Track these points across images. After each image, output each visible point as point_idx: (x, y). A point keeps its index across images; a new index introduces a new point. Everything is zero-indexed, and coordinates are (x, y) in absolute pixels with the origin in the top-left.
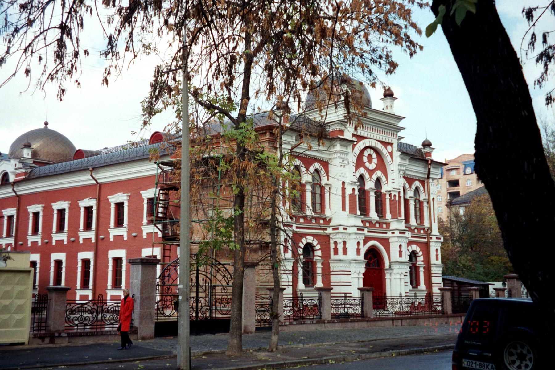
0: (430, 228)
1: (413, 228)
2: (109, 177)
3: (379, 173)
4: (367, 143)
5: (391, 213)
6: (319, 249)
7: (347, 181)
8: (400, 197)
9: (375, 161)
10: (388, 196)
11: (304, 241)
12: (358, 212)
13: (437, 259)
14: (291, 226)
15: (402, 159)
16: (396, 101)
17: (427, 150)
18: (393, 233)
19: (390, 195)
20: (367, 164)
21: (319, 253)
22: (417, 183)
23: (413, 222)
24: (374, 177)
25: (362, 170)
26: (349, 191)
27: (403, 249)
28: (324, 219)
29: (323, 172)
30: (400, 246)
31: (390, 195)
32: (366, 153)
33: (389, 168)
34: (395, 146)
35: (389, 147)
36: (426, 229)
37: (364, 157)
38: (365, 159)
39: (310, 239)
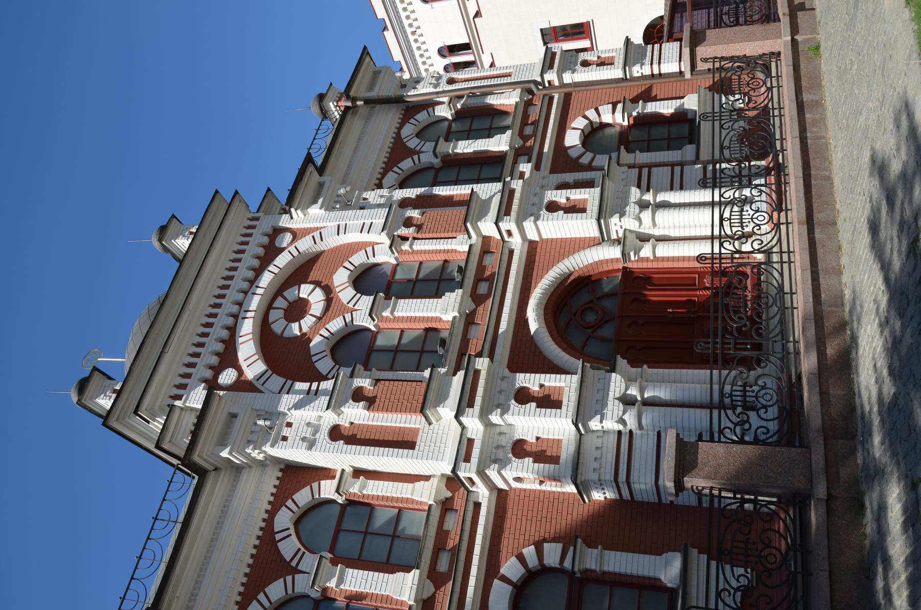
1: (518, 143)
4: (247, 327)
7: (330, 418)
15: (314, 202)
18: (509, 233)
22: (408, 130)
24: (346, 294)
28: (446, 506)
29: (303, 497)
33: (332, 241)
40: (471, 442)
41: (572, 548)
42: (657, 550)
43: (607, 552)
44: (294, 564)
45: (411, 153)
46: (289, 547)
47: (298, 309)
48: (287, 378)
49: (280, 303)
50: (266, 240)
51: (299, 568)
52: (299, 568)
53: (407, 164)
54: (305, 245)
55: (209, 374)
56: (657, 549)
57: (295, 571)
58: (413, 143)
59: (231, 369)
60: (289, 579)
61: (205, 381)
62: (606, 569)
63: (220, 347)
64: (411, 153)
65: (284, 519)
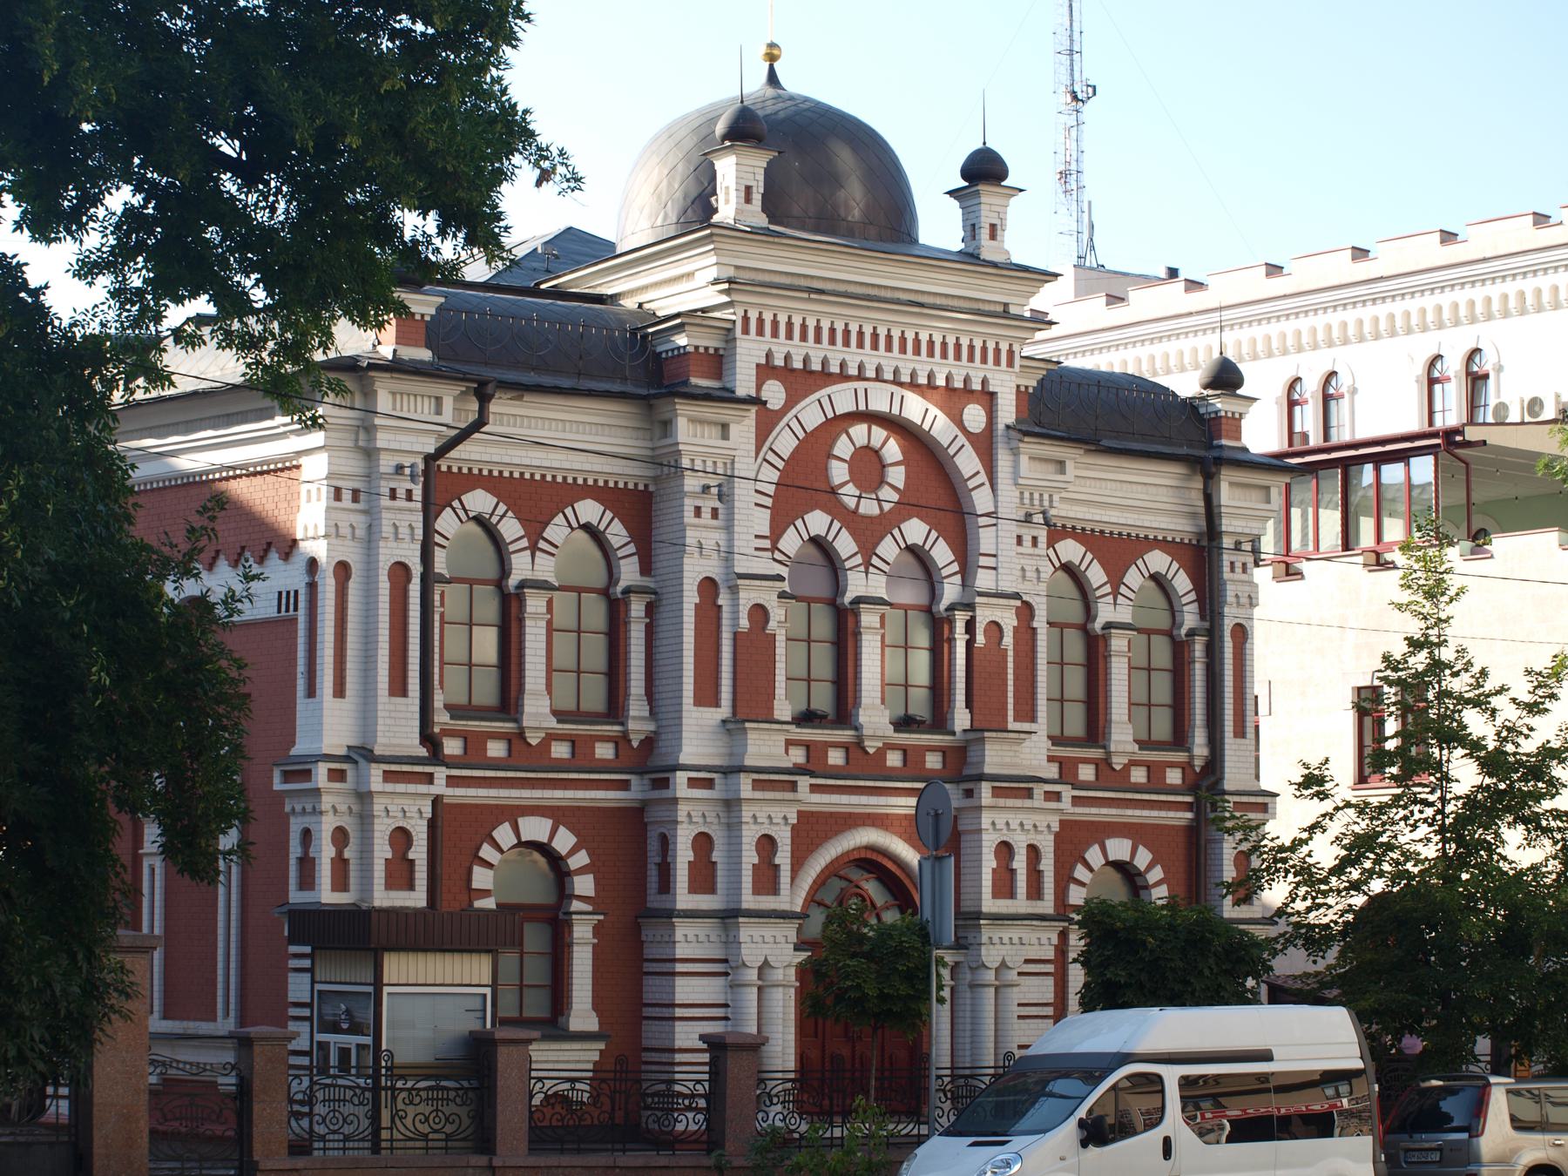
0: (1215, 763)
1: (1118, 762)
3: (915, 530)
4: (843, 398)
5: (969, 704)
6: (582, 871)
8: (1026, 632)
9: (897, 476)
10: (960, 627)
14: (429, 779)
16: (1015, 202)
17: (1221, 404)
19: (970, 626)
21: (584, 885)
22: (1158, 561)
23: (1122, 737)
25: (817, 521)
27: (1020, 863)
30: (1005, 850)
31: (970, 626)
34: (1007, 412)
35: (975, 416)
36: (1198, 763)
37: (834, 464)
38: (839, 473)
39: (535, 828)
40: (708, 784)
41: (590, 908)
42: (596, 1006)
43: (590, 949)
44: (542, 544)
46: (556, 531)
47: (868, 466)
48: (775, 497)
49: (879, 434)
50: (976, 386)
51: (538, 553)
52: (538, 553)
53: (1096, 575)
54: (968, 462)
55: (779, 362)
56: (598, 1005)
57: (534, 548)
58: (1133, 578)
59: (783, 396)
60: (525, 543)
61: (769, 355)
62: (575, 948)
63: (816, 366)
65: (589, 510)
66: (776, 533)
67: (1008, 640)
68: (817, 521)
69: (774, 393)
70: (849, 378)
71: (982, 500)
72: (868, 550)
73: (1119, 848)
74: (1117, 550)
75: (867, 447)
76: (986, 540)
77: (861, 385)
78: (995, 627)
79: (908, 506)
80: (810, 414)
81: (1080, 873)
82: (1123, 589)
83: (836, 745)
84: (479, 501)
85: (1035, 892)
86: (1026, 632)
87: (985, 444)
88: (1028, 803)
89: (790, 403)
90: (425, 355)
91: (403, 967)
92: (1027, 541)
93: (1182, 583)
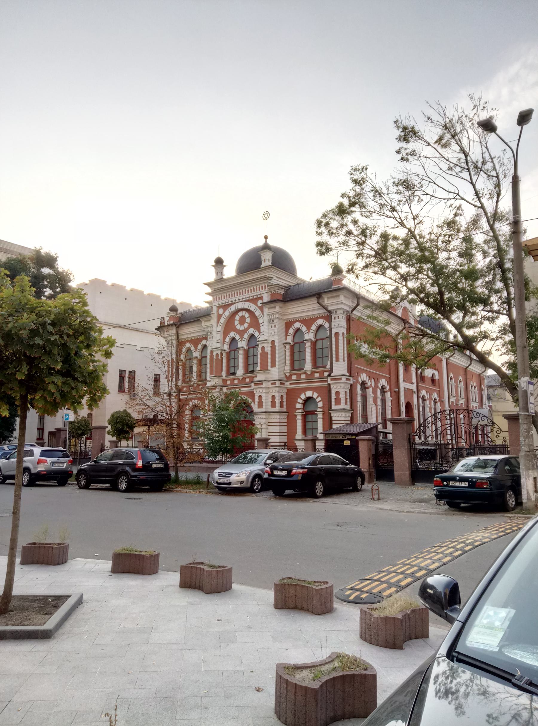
2: (344, 353)
3: (251, 331)
4: (233, 308)
8: (273, 348)
9: (248, 320)
11: (191, 404)
12: (224, 373)
13: (346, 404)
20: (238, 327)
24: (246, 336)
25: (232, 334)
26: (215, 357)
32: (237, 317)
38: (236, 322)
45: (309, 329)
47: (242, 321)
49: (244, 312)
54: (258, 313)
64: (309, 329)
66: (224, 338)
67: (268, 349)
68: (232, 334)
69: (221, 311)
70: (235, 303)
71: (260, 321)
72: (242, 337)
73: (309, 394)
74: (308, 322)
75: (243, 316)
76: (262, 329)
77: (236, 304)
78: (263, 348)
79: (250, 326)
80: (227, 313)
81: (300, 401)
82: (311, 331)
83: (229, 380)
84: (188, 345)
85: (282, 406)
86: (273, 348)
87: (261, 309)
88: (262, 386)
89: (224, 312)
90: (171, 322)
91: (355, 429)
92: (273, 326)
93: (327, 325)
